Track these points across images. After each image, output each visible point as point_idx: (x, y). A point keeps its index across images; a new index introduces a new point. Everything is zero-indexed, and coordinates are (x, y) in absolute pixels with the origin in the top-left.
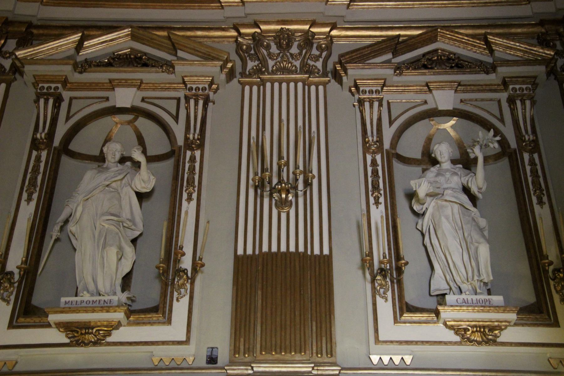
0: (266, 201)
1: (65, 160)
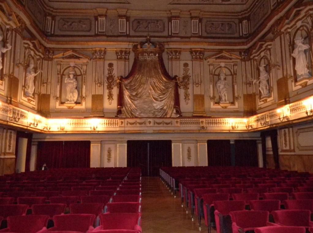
0: (97, 85)
1: (63, 76)
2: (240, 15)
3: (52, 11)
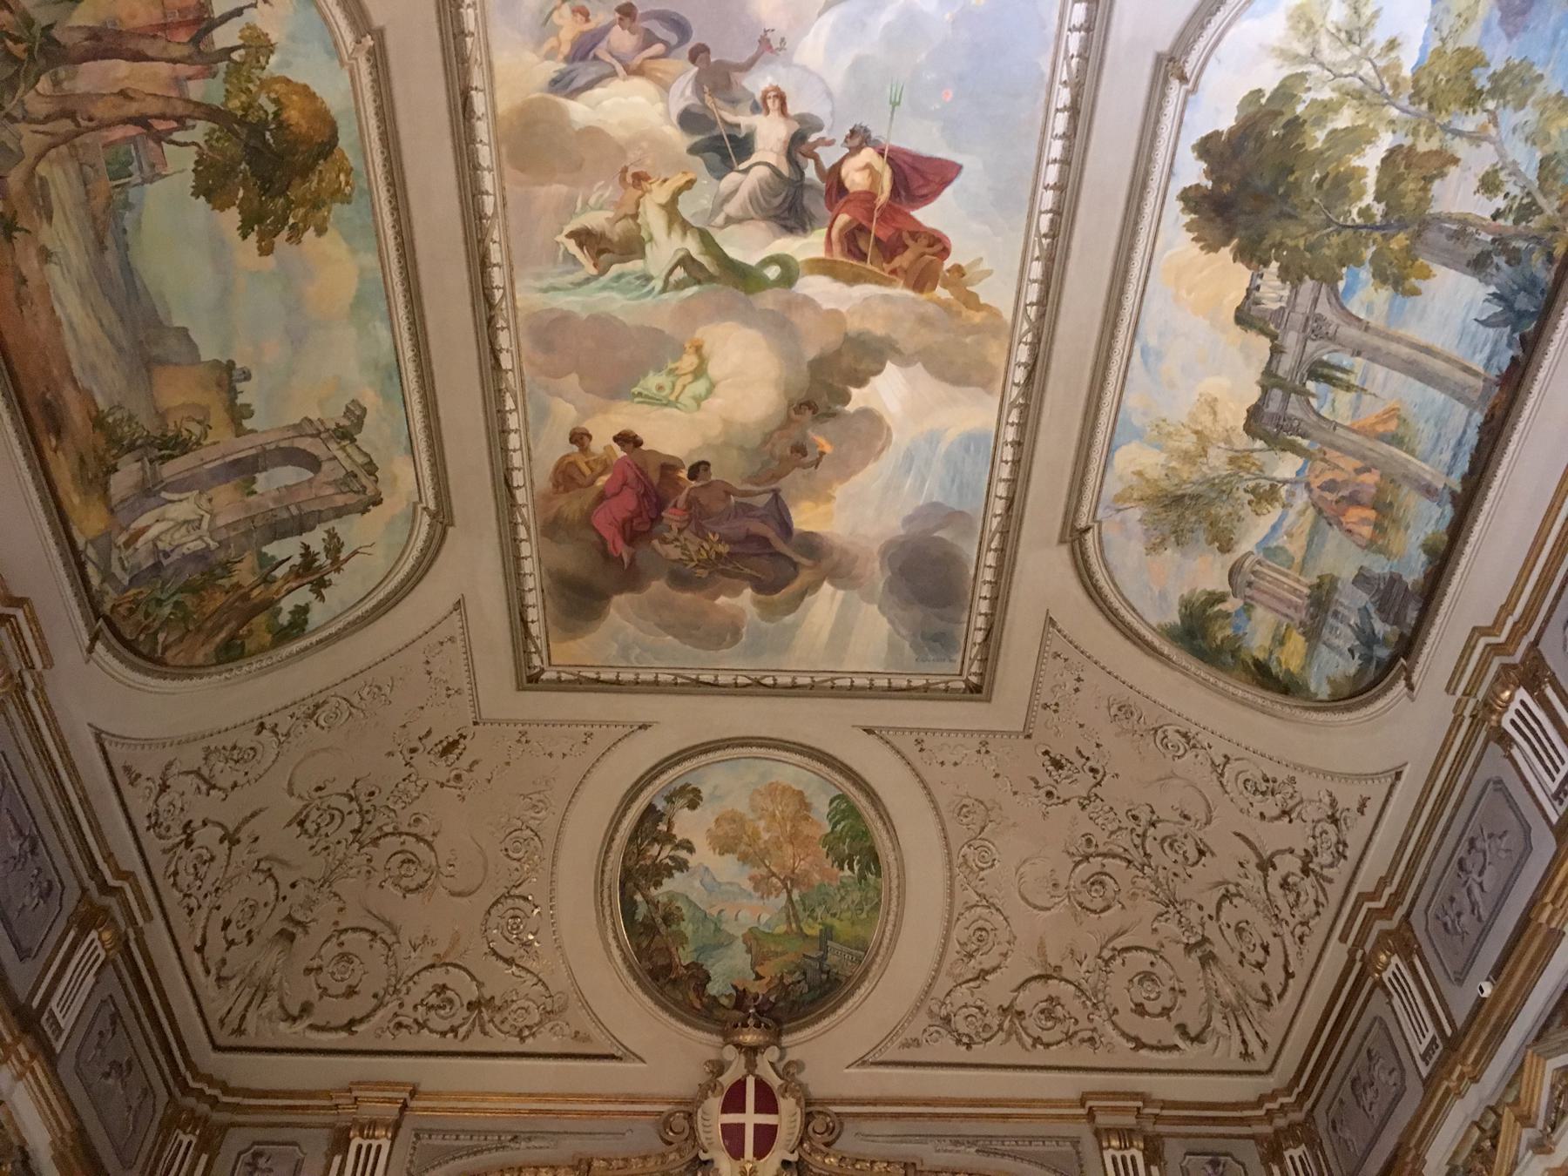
2: (1259, 1119)
3: (214, 1102)
